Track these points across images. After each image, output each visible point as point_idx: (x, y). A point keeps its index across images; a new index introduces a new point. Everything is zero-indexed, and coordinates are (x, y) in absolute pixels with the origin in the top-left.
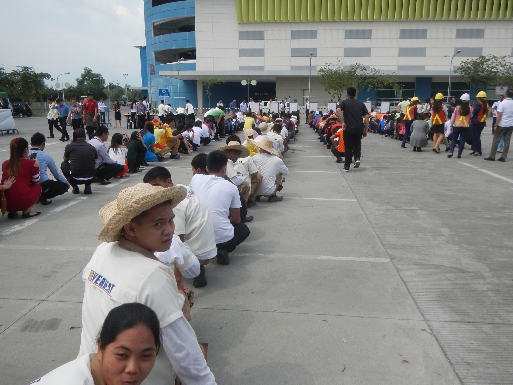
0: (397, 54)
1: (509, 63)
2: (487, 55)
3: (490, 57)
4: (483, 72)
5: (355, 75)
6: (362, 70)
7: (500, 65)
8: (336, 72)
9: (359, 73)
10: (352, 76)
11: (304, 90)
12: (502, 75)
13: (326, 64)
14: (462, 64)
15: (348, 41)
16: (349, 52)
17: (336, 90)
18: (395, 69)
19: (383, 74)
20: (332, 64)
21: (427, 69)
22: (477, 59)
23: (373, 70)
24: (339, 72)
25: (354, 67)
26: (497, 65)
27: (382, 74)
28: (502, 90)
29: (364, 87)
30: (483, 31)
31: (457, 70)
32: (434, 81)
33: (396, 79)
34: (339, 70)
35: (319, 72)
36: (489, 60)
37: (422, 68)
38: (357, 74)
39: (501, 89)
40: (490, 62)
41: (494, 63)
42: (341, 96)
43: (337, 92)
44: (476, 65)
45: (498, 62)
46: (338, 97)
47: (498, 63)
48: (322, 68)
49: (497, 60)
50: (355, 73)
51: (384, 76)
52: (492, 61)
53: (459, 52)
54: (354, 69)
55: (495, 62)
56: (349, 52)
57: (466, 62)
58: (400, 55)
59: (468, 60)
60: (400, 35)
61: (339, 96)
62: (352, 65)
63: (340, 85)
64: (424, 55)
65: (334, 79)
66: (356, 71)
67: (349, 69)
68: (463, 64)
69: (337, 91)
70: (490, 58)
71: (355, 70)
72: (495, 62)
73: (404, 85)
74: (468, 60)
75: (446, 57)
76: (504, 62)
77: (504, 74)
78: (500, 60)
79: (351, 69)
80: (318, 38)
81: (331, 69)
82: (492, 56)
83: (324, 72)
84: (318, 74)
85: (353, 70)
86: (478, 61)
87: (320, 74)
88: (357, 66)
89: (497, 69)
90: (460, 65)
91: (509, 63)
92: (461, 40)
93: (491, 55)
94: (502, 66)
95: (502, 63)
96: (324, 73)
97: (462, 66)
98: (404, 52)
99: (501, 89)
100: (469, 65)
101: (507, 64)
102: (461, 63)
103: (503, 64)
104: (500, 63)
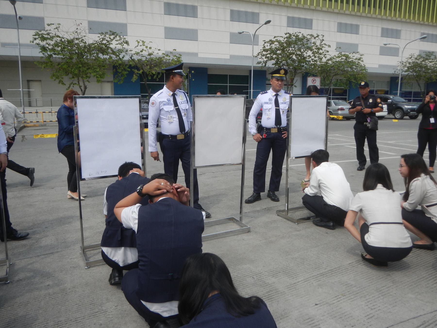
0: (163, 36)
8: (70, 42)
11: (28, 81)
14: (266, 45)
15: (93, 11)
17: (76, 79)
19: (159, 50)
20: (60, 26)
22: (287, 38)
23: (141, 43)
24: (77, 42)
28: (314, 83)
29: (126, 74)
30: (258, 14)
31: (262, 52)
32: (210, 72)
34: (77, 39)
35: (35, 39)
37: (196, 54)
39: (313, 80)
42: (86, 88)
43: (79, 82)
46: (82, 90)
54: (107, 40)
57: (271, 41)
60: (165, 10)
61: (83, 88)
69: (78, 79)
73: (193, 72)
79: (101, 40)
80: (44, 2)
81: (61, 36)
84: (33, 42)
85: (104, 42)
90: (264, 45)
97: (264, 47)
99: (313, 80)
102: (265, 43)
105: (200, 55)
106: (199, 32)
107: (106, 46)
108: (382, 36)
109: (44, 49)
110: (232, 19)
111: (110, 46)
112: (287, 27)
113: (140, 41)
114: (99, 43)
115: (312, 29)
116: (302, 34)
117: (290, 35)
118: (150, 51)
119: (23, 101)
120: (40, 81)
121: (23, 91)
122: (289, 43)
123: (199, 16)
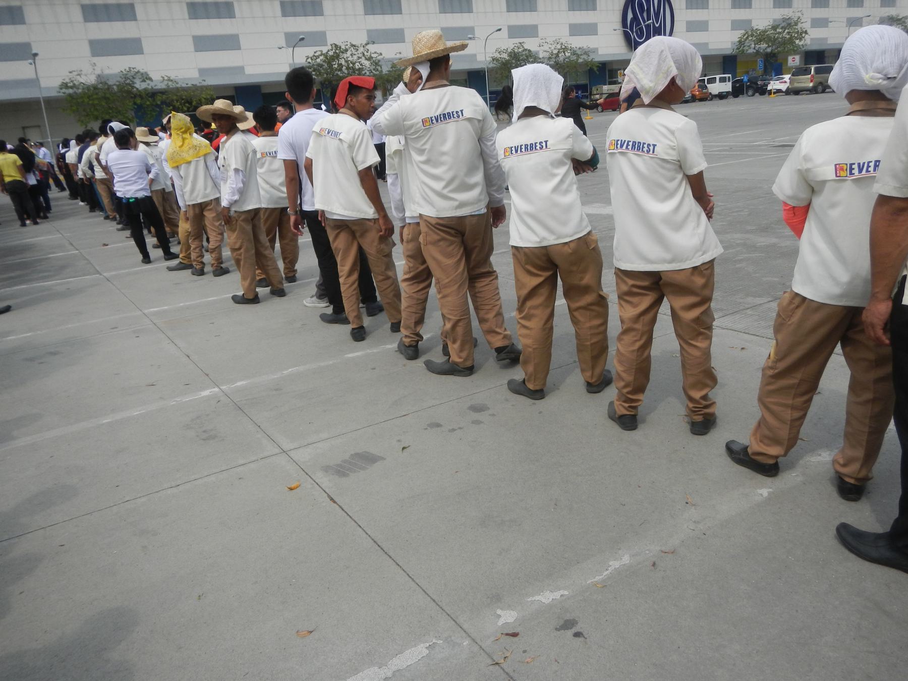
0: (192, 49)
1: (375, 53)
2: (342, 43)
3: (347, 45)
4: (340, 70)
5: (135, 89)
6: (144, 81)
7: (363, 58)
8: (95, 88)
9: (140, 85)
10: (129, 92)
11: (24, 128)
12: (370, 73)
13: (70, 72)
15: (93, 26)
16: (99, 48)
18: (196, 74)
19: (187, 84)
21: (249, 71)
22: (329, 51)
23: (166, 78)
24: (100, 86)
25: (126, 74)
26: (359, 58)
27: (184, 85)
33: (211, 93)
34: (101, 83)
35: (61, 89)
36: (346, 50)
37: (241, 69)
38: (137, 89)
40: (349, 53)
41: (355, 54)
44: (330, 60)
45: (361, 53)
47: (360, 55)
48: (64, 82)
49: (358, 50)
50: (133, 87)
51: (184, 89)
52: (351, 53)
53: (302, 39)
55: (356, 53)
56: (99, 48)
57: (314, 56)
58: (197, 49)
59: (315, 53)
60: (189, 14)
62: (121, 71)
63: (111, 111)
64: (238, 48)
65: (96, 102)
66: (134, 84)
67: (120, 79)
68: (309, 60)
70: (347, 47)
71: (131, 81)
72: (356, 53)
74: (315, 53)
75: (280, 48)
76: (367, 52)
77: (372, 72)
78: (361, 50)
79: (124, 79)
82: (349, 43)
83: (71, 87)
85: (128, 81)
86: (331, 53)
87: (64, 93)
88: (132, 73)
89: (361, 65)
90: (306, 61)
91: (375, 53)
92: (291, 19)
93: (347, 42)
94: (366, 59)
95: (366, 54)
96: (71, 91)
97: (309, 63)
98: (202, 44)
100: (318, 60)
101: (373, 55)
102: (307, 59)
103: (367, 55)
104: (364, 54)
105: (249, 71)
106: (241, 36)
107: (131, 86)
108: (508, 11)
109: (70, 95)
110: (285, 14)
111: (135, 85)
112: (365, 15)
113: (165, 77)
114: (123, 84)
115: (401, 13)
116: (350, 43)
117: (336, 45)
118: (178, 86)
119: (54, 151)
120: (39, 126)
121: (51, 140)
122: (336, 57)
123: (237, 16)
